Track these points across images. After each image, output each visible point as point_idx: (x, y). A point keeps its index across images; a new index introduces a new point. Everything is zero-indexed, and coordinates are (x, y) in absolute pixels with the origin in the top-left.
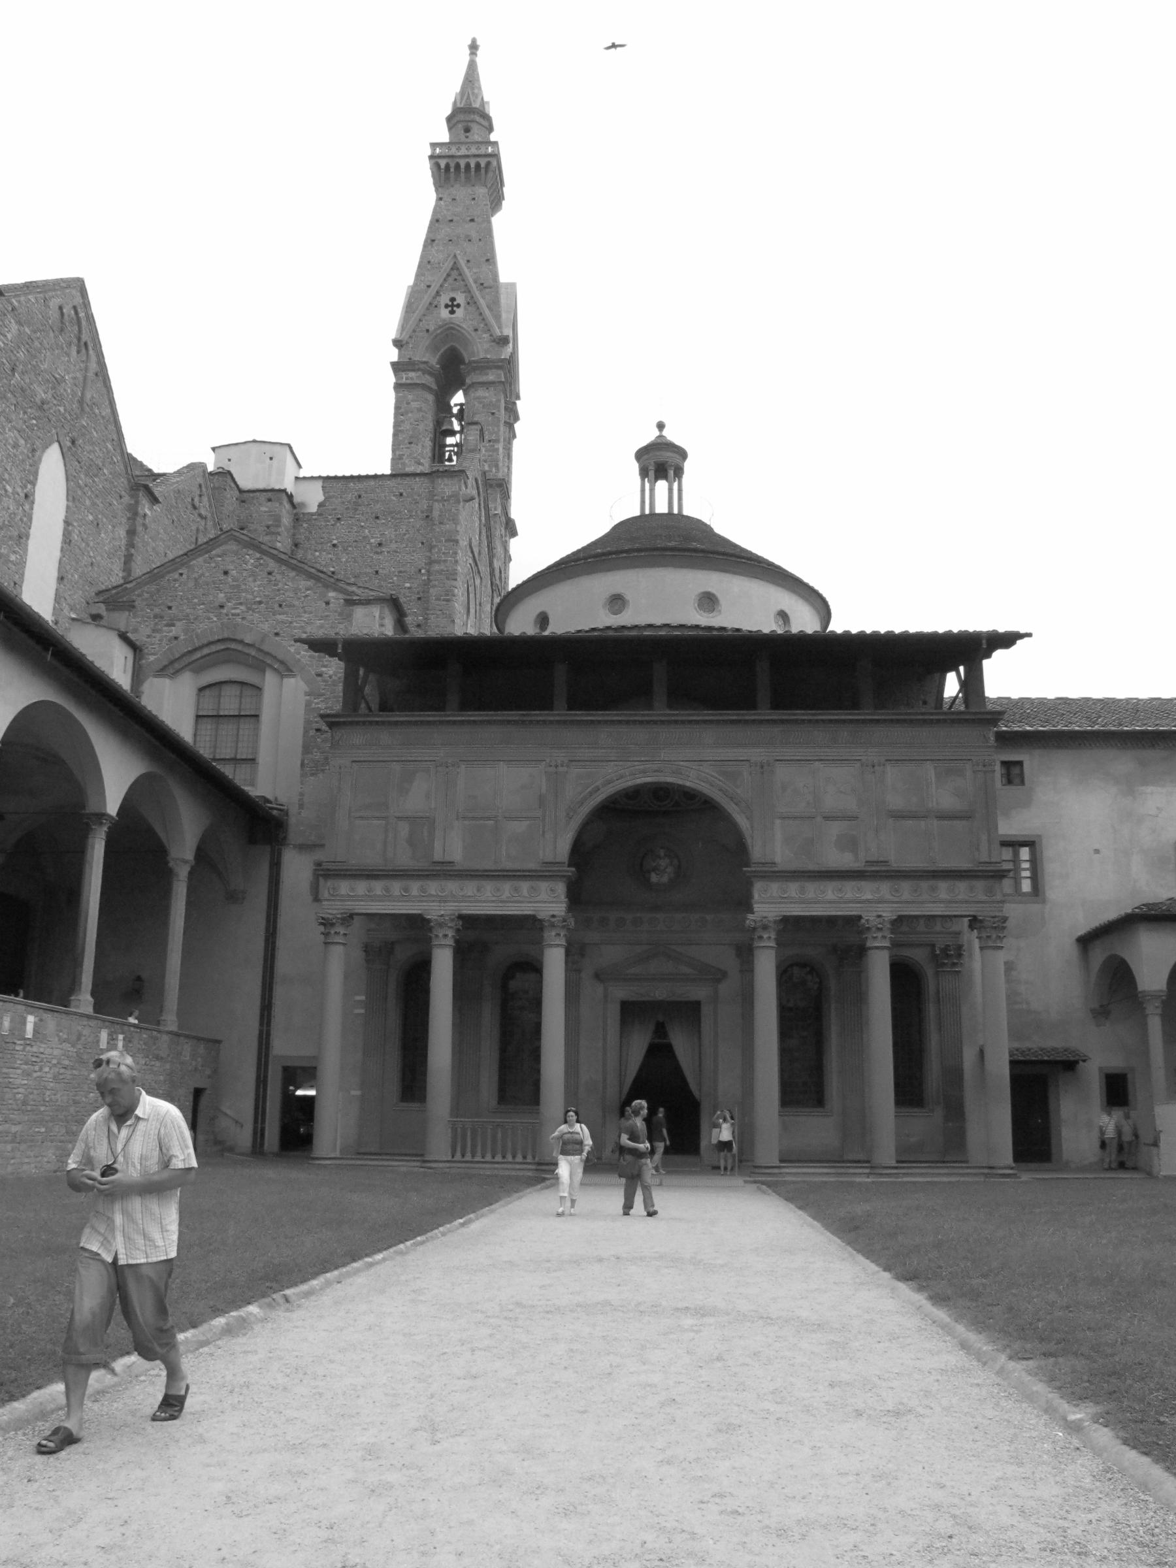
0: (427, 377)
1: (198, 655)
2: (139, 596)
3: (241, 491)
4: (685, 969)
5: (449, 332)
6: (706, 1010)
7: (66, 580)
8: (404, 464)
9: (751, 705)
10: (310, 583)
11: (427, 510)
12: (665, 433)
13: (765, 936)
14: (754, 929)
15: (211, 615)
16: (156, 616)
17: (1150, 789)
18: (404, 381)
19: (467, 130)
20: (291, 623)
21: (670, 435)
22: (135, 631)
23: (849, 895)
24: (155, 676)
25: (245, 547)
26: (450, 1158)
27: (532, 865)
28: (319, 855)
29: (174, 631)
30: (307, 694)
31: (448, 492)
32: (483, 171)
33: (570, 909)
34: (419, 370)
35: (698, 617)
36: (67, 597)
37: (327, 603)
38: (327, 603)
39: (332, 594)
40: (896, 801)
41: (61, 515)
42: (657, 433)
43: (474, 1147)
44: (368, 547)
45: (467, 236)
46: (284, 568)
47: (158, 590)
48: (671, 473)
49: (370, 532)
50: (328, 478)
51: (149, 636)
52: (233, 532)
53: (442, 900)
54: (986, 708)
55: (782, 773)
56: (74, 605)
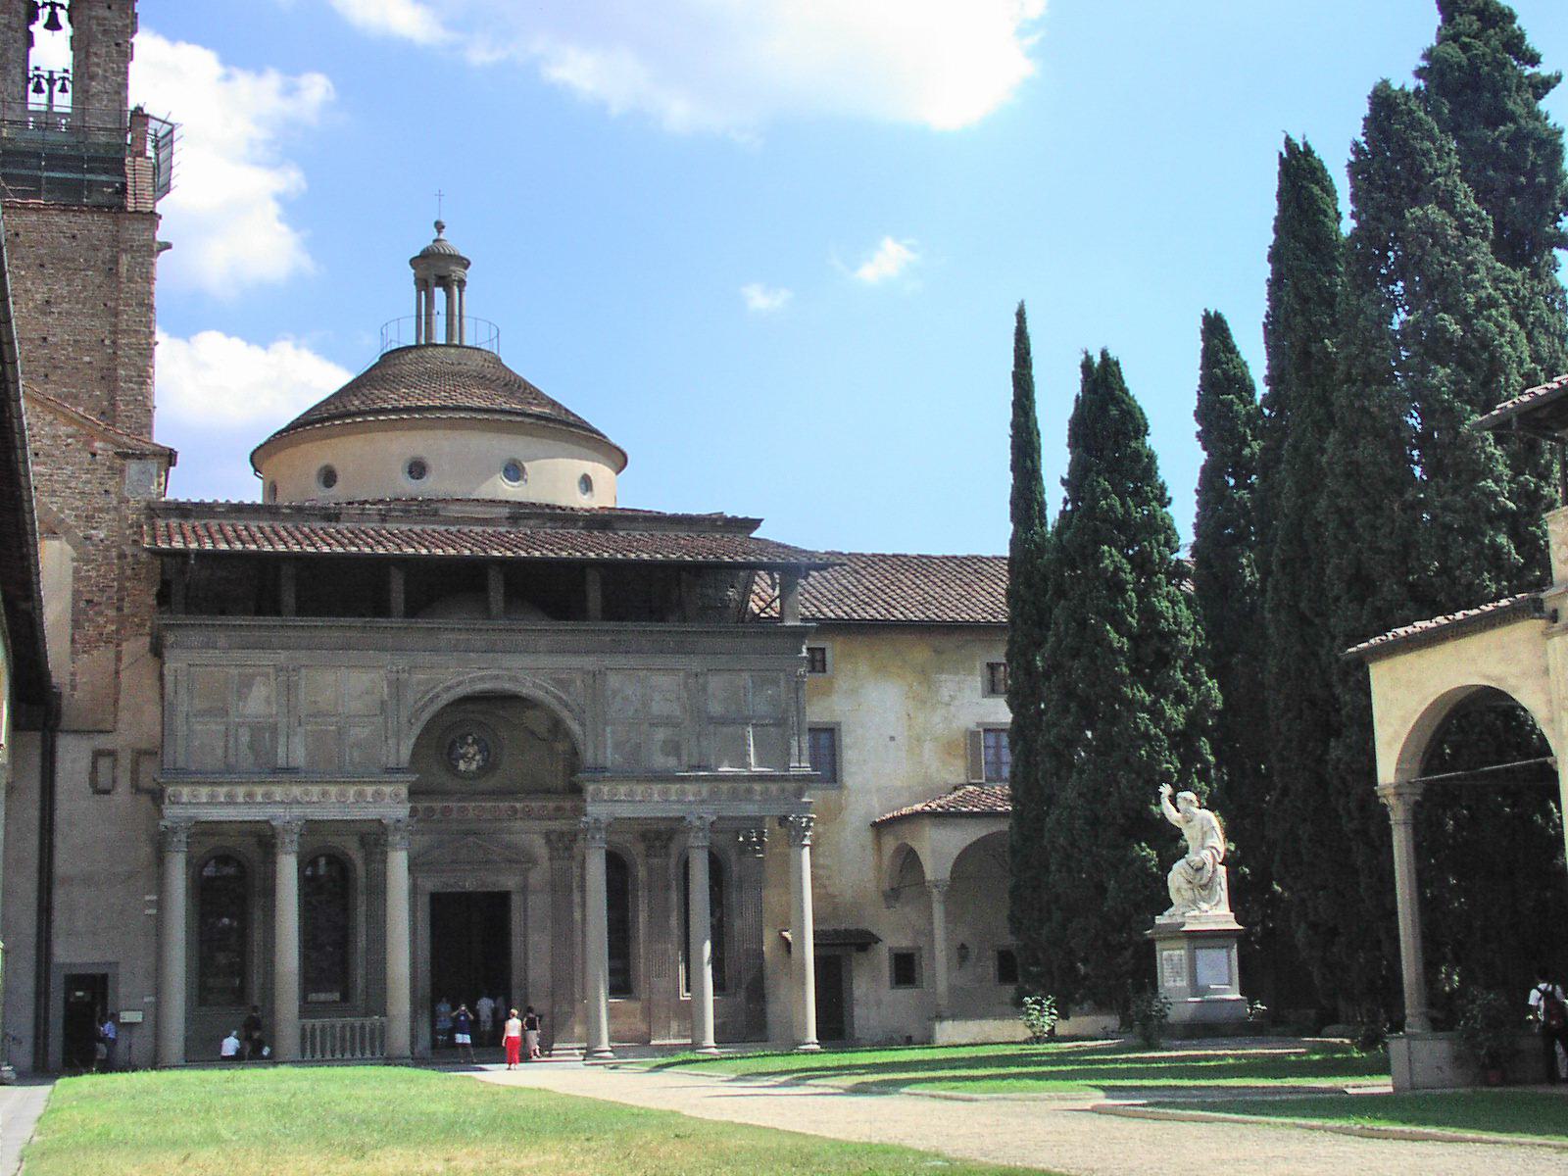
6: (516, 901)
10: (70, 430)
11: (110, 261)
17: (944, 677)
28: (102, 742)
30: (73, 560)
37: (94, 455)
38: (94, 455)
39: (98, 444)
40: (716, 708)
43: (323, 1044)
44: (31, 304)
46: (38, 409)
49: (33, 284)
55: (614, 681)
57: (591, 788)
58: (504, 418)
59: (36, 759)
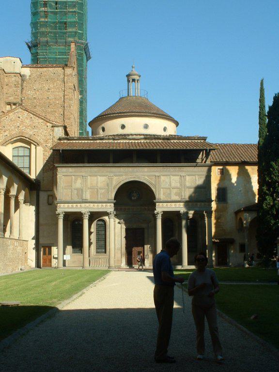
6: (146, 231)
10: (42, 121)
23: (177, 206)
27: (106, 200)
28: (49, 193)
33: (114, 210)
39: (48, 124)
48: (136, 82)
53: (85, 208)
55: (162, 178)
57: (157, 204)
58: (143, 114)
59: (35, 197)
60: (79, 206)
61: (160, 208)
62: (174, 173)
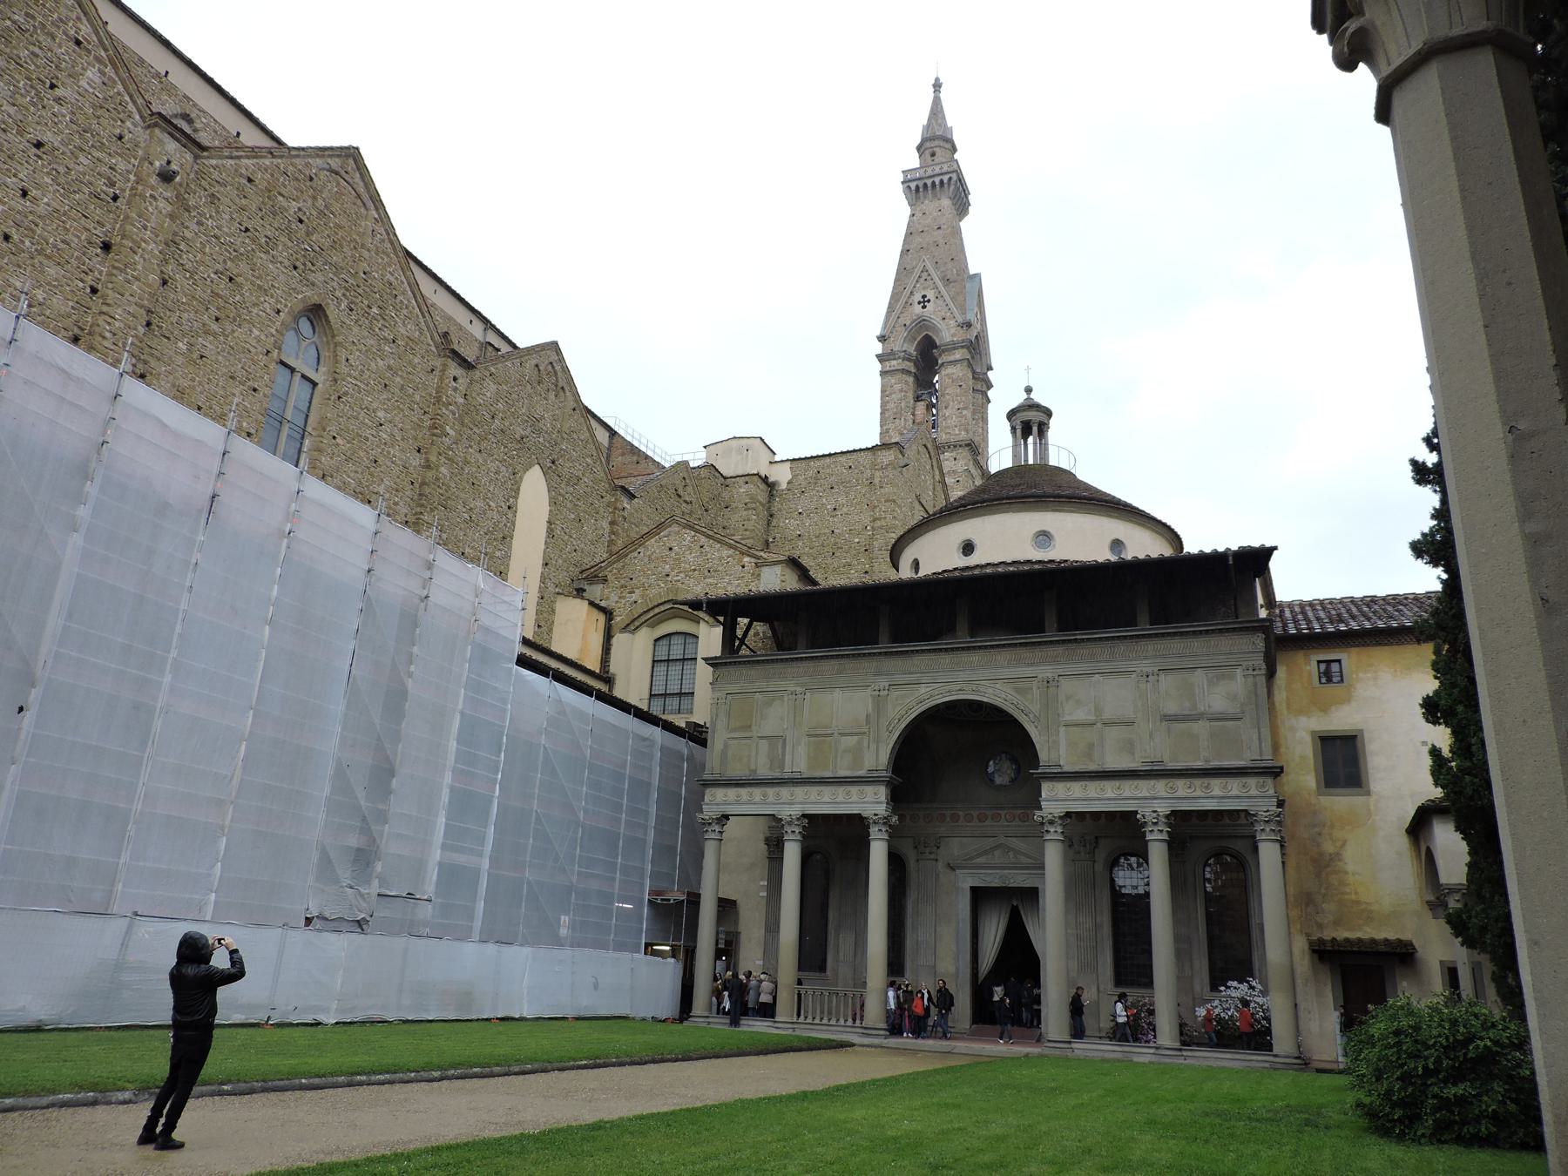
0: (908, 363)
1: (651, 614)
2: (610, 572)
3: (725, 478)
4: (1024, 860)
5: (922, 323)
7: (549, 566)
8: (890, 437)
9: (1040, 629)
12: (1032, 396)
13: (1052, 830)
14: (1042, 824)
15: (660, 583)
16: (622, 587)
18: (888, 368)
19: (933, 155)
20: (716, 584)
21: (1037, 397)
22: (608, 598)
23: (1127, 794)
24: (621, 632)
25: (684, 528)
26: (795, 1020)
29: (634, 597)
31: (886, 462)
32: (946, 186)
34: (899, 358)
35: (1036, 553)
36: (552, 577)
37: (743, 567)
38: (743, 567)
39: (746, 559)
40: (1172, 707)
41: (546, 517)
42: (1026, 396)
45: (935, 242)
46: (711, 541)
47: (624, 566)
48: (1035, 429)
50: (794, 460)
51: (617, 602)
52: (675, 517)
54: (1258, 615)
56: (560, 583)
60: (771, 799)
61: (1056, 799)
62: (1107, 667)
